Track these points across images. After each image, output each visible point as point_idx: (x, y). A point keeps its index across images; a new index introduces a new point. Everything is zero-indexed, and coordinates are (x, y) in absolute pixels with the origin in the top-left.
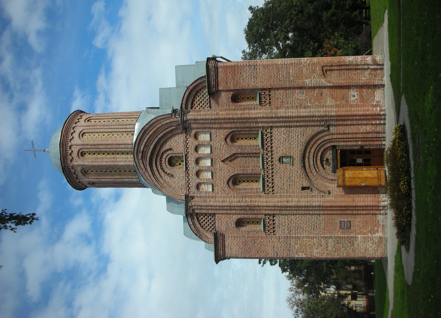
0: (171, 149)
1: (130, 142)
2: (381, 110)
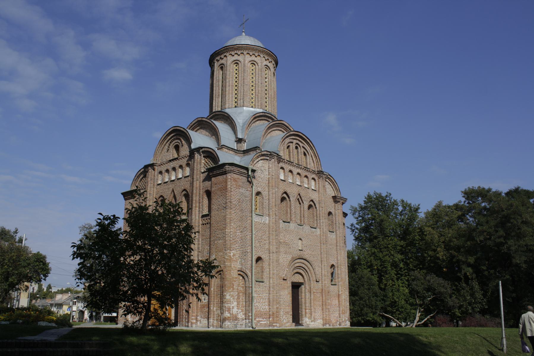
0: (182, 146)
1: (227, 106)
2: (192, 323)
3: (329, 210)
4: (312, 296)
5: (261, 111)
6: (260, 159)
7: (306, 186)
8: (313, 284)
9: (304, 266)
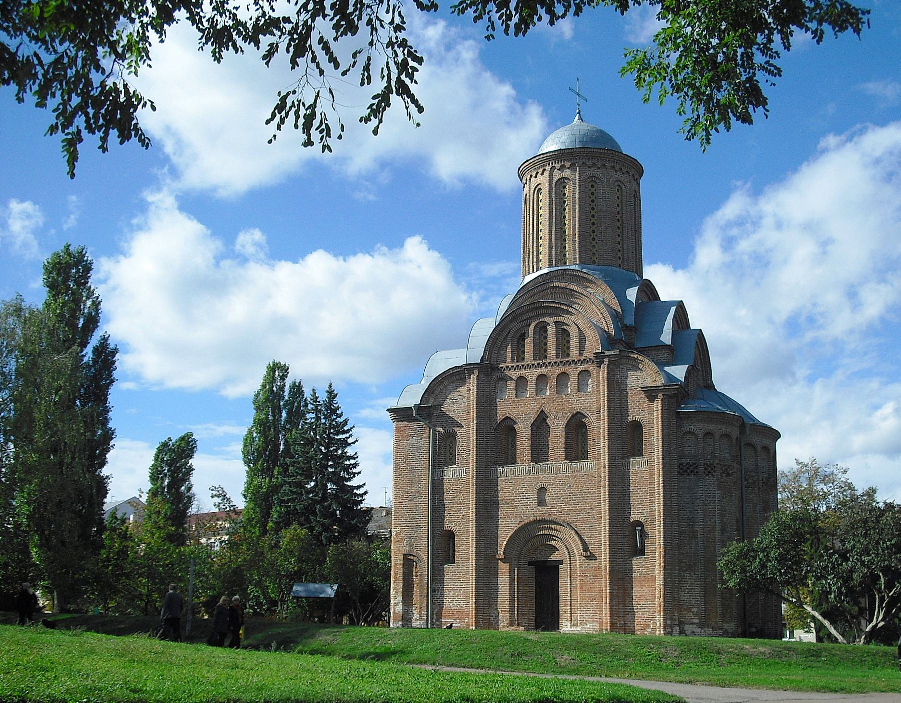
3: (630, 418)
5: (545, 271)
6: (446, 383)
8: (578, 560)
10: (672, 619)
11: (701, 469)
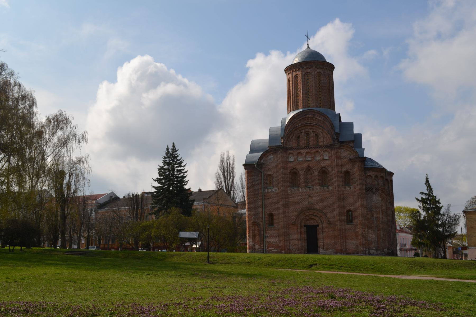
3: (344, 170)
4: (324, 234)
5: (301, 110)
6: (268, 154)
7: (318, 158)
9: (315, 214)
10: (365, 248)
11: (374, 190)
